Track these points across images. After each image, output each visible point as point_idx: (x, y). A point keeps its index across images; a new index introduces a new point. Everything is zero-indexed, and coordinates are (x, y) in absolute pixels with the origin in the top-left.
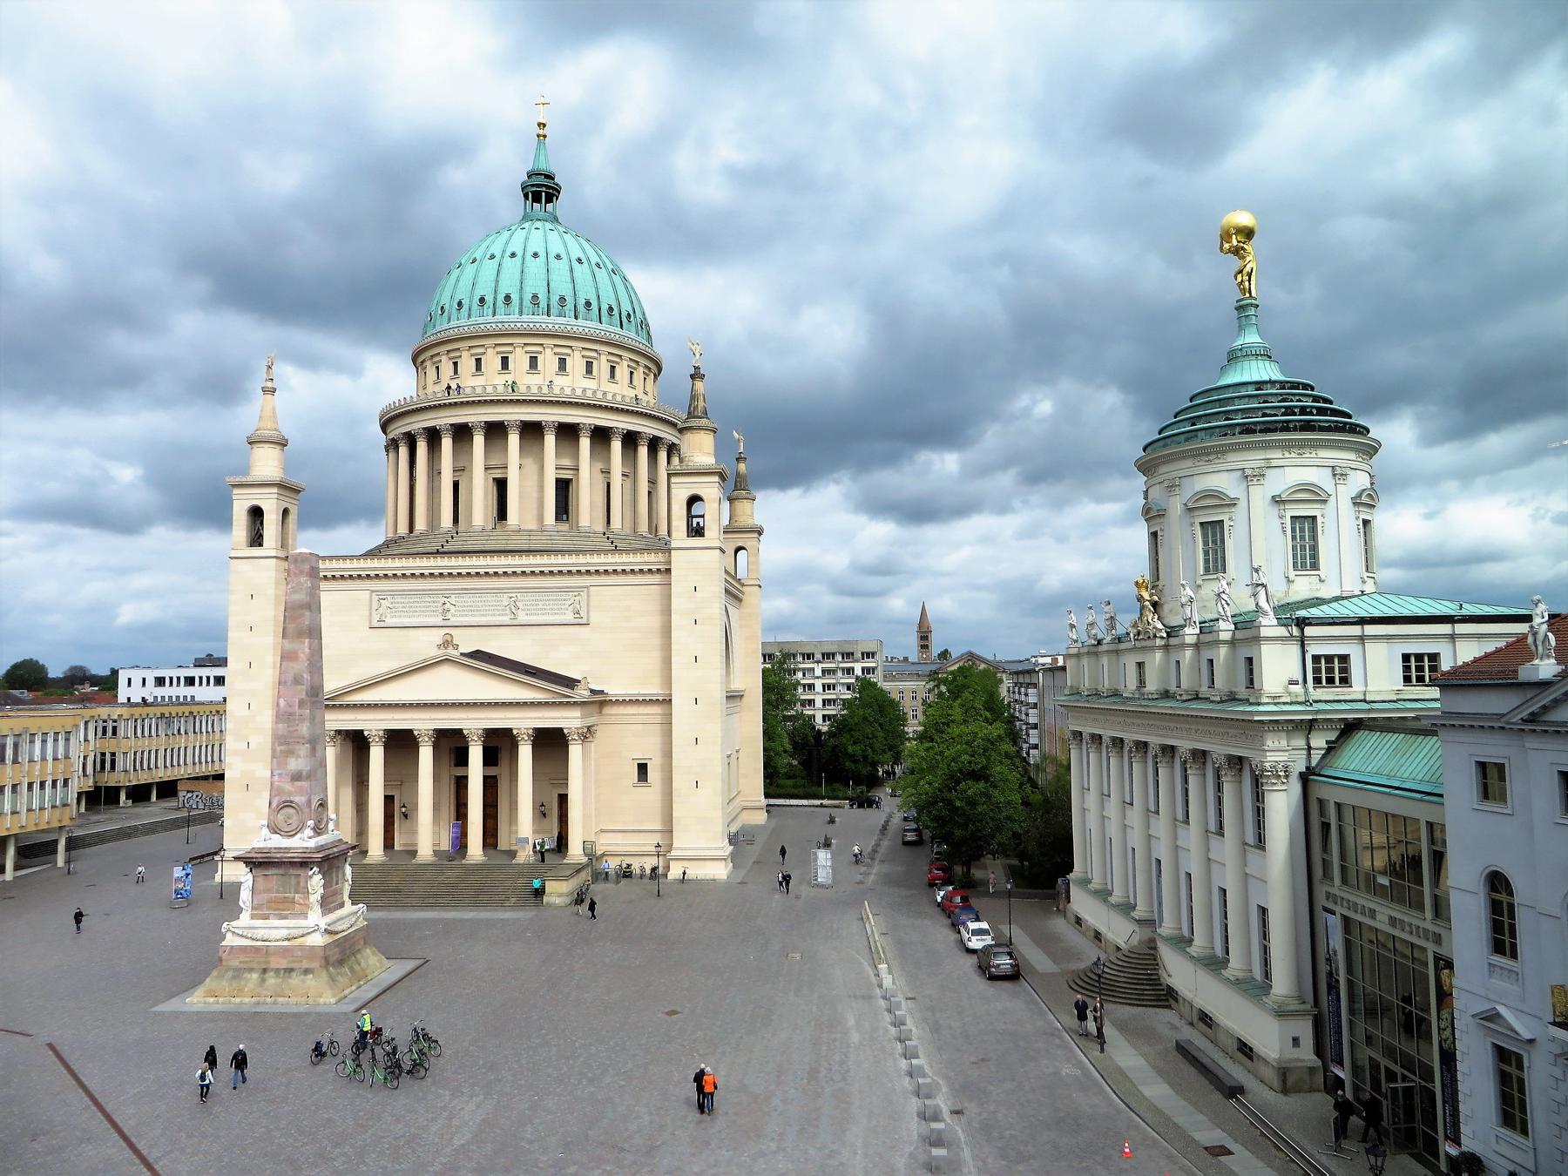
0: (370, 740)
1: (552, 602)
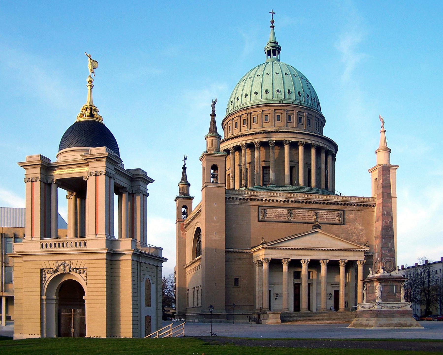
0: (283, 263)
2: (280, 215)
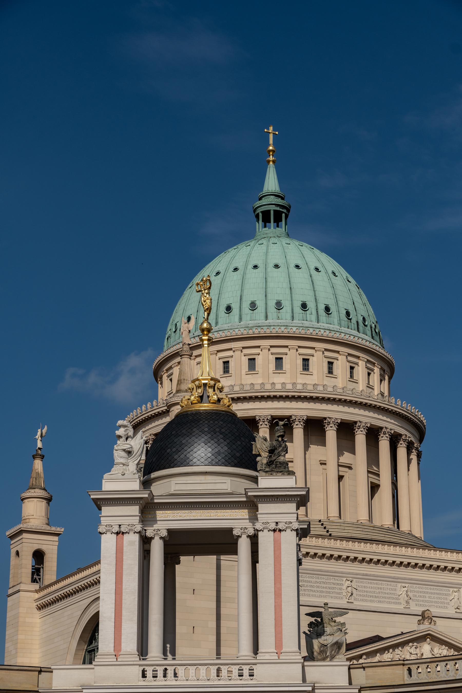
1: (436, 596)
2: (329, 590)
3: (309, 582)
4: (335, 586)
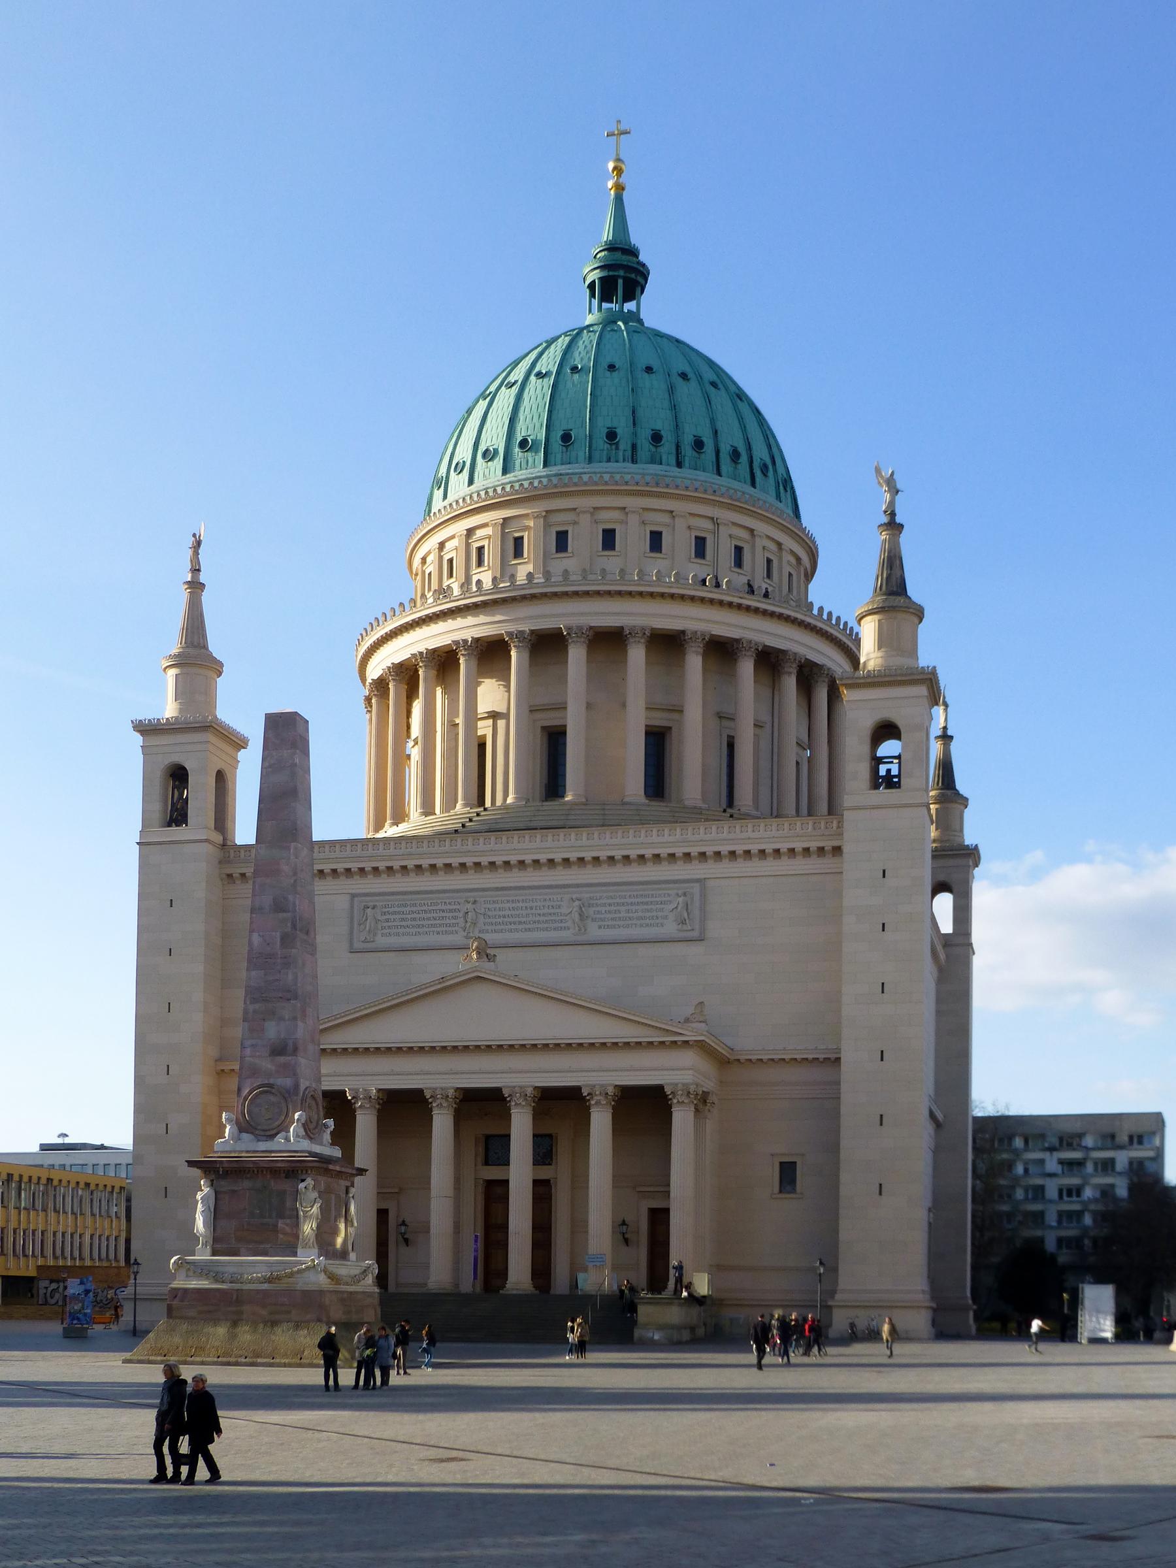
3: (399, 913)
4: (444, 914)
